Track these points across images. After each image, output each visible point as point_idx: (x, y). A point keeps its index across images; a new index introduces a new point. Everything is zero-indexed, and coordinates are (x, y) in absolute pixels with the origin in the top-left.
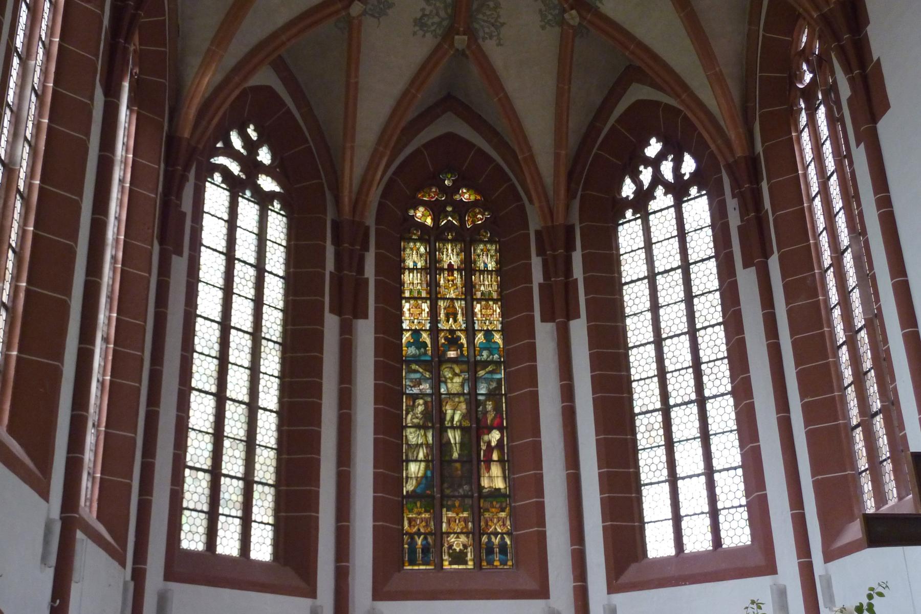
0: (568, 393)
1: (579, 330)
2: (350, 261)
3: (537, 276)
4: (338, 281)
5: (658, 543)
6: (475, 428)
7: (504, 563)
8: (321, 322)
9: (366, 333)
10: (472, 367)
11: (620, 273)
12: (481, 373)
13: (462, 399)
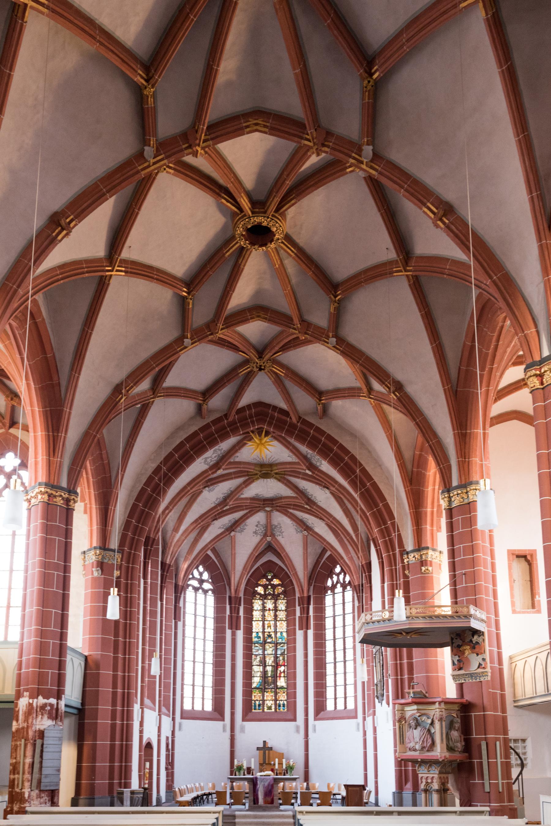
0: (306, 655)
1: (311, 633)
2: (235, 610)
4: (231, 617)
5: (330, 706)
6: (276, 666)
7: (284, 710)
9: (240, 634)
10: (276, 644)
11: (325, 613)
12: (279, 647)
13: (272, 656)
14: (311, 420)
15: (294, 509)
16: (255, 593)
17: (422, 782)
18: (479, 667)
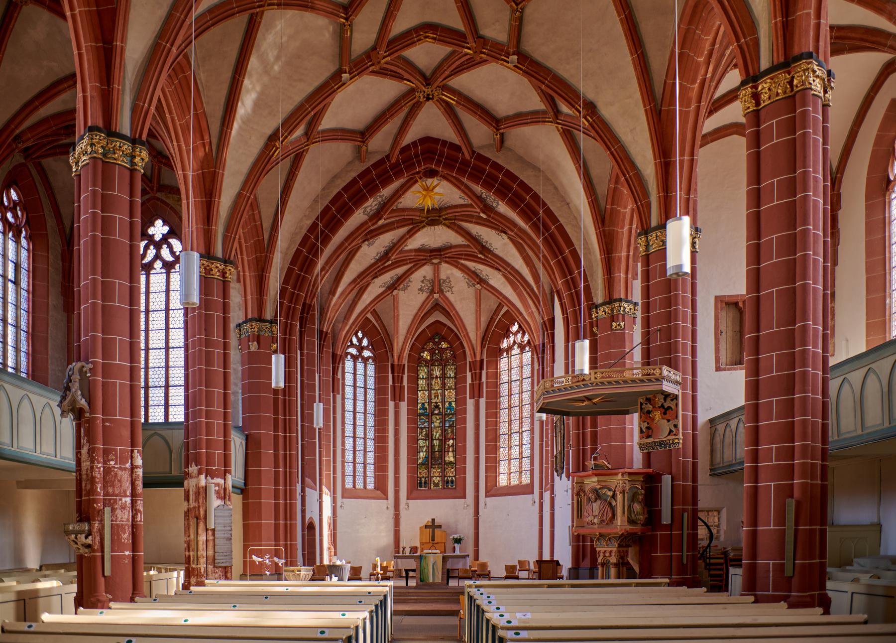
0: (477, 427)
1: (483, 401)
2: (398, 380)
3: (469, 381)
4: (394, 387)
8: (386, 404)
9: (404, 406)
10: (443, 416)
14: (488, 154)
15: (465, 259)
16: (421, 358)
18: (669, 434)
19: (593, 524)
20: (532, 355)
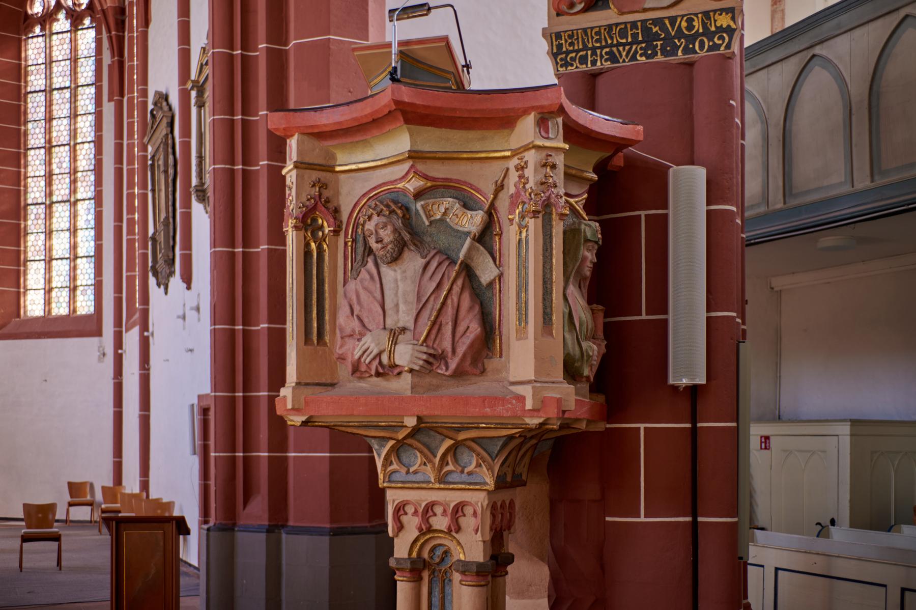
5: (34, 306)
17: (400, 527)
19: (388, 370)
20: (99, 32)
